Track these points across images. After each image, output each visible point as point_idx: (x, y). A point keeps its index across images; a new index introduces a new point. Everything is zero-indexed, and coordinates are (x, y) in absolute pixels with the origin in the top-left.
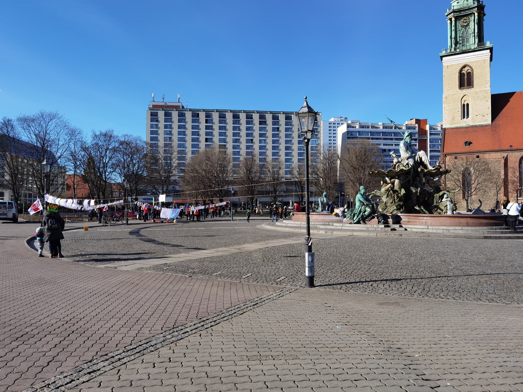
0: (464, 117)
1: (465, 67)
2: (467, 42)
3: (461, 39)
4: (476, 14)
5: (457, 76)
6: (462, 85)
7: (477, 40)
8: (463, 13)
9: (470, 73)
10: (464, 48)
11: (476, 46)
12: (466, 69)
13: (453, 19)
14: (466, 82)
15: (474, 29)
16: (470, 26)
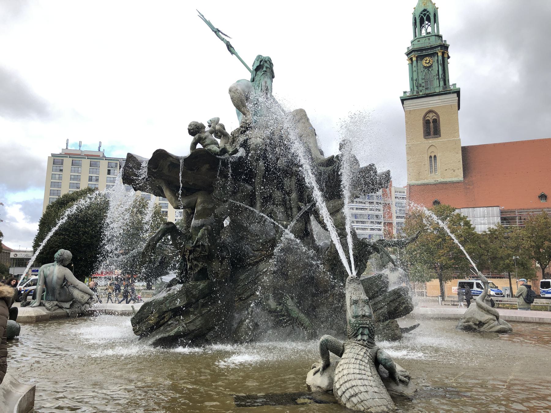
1: (430, 111)
5: (421, 122)
7: (442, 83)
8: (424, 53)
10: (428, 92)
11: (441, 89)
12: (431, 115)
13: (414, 59)
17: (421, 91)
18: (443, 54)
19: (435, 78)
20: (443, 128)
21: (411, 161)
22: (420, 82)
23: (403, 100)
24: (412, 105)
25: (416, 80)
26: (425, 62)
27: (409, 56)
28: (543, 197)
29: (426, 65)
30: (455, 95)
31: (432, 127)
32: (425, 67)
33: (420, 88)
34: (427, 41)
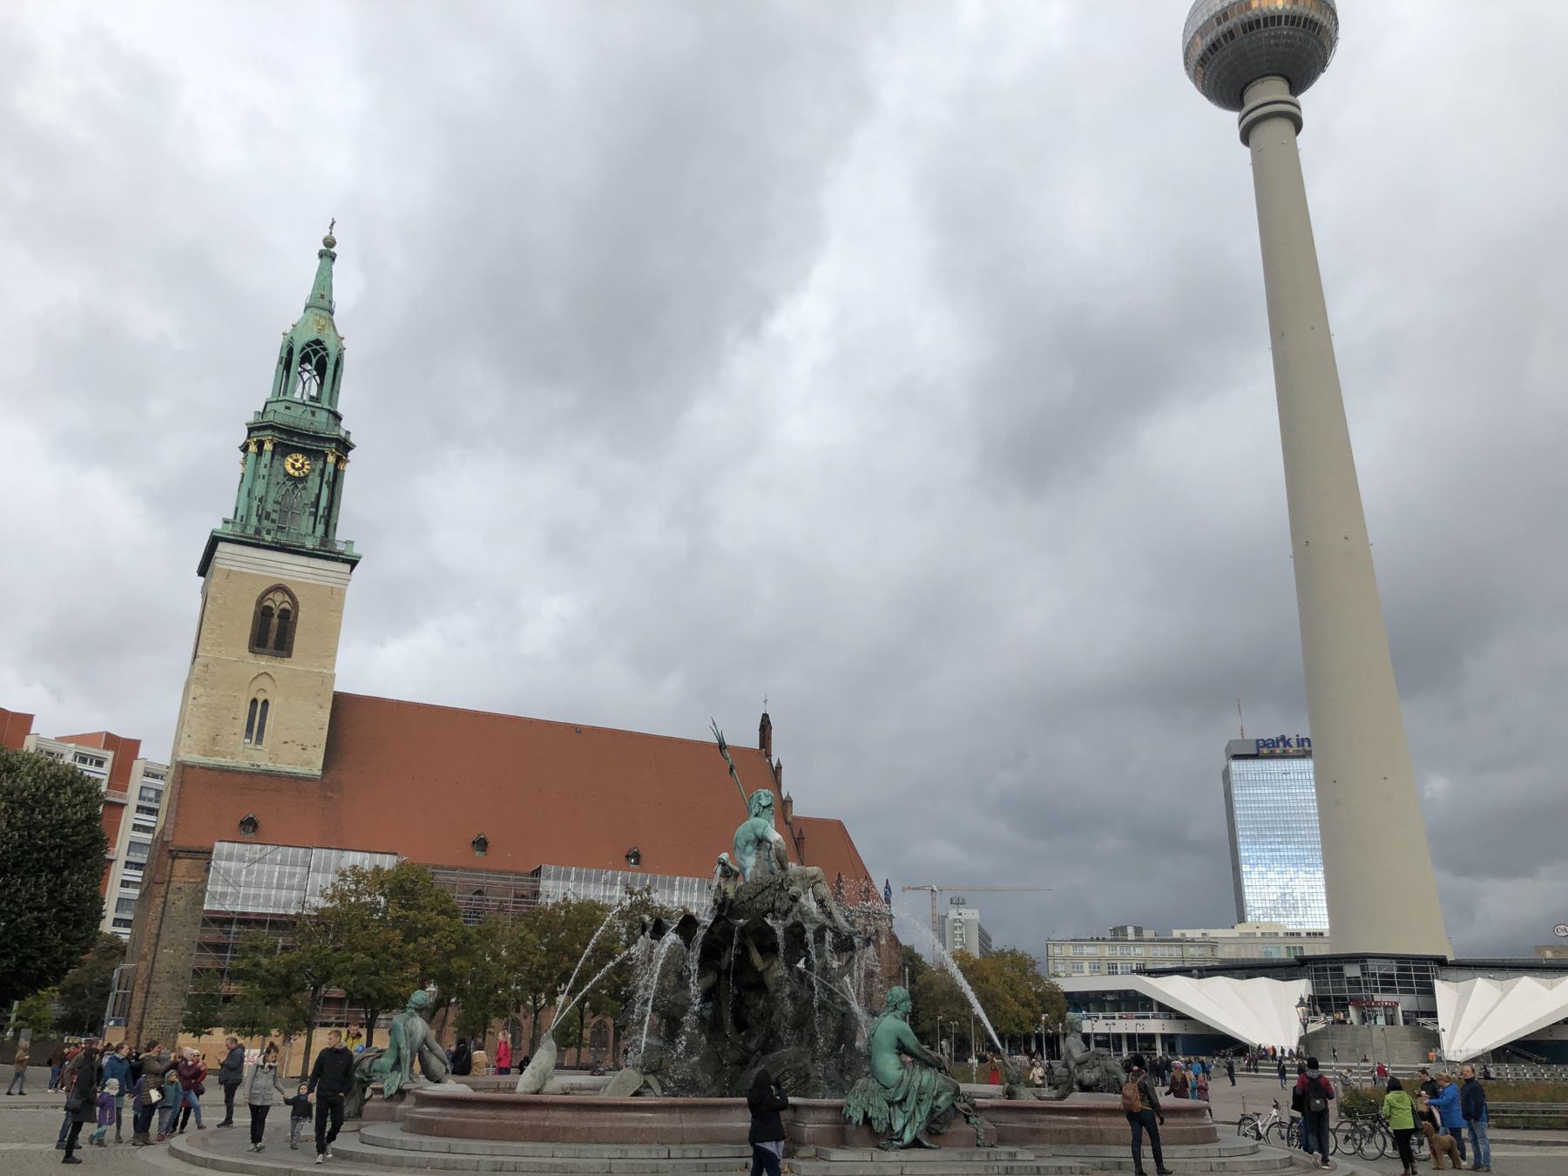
1: (280, 588)
6: (259, 642)
7: (320, 529)
10: (282, 538)
13: (268, 447)
14: (273, 636)
15: (318, 496)
16: (309, 484)
17: (268, 533)
18: (339, 460)
20: (300, 640)
21: (201, 700)
22: (270, 507)
23: (214, 541)
25: (261, 500)
26: (294, 464)
27: (255, 433)
28: (481, 844)
29: (292, 471)
31: (274, 629)
32: (287, 474)
33: (266, 523)
34: (308, 416)
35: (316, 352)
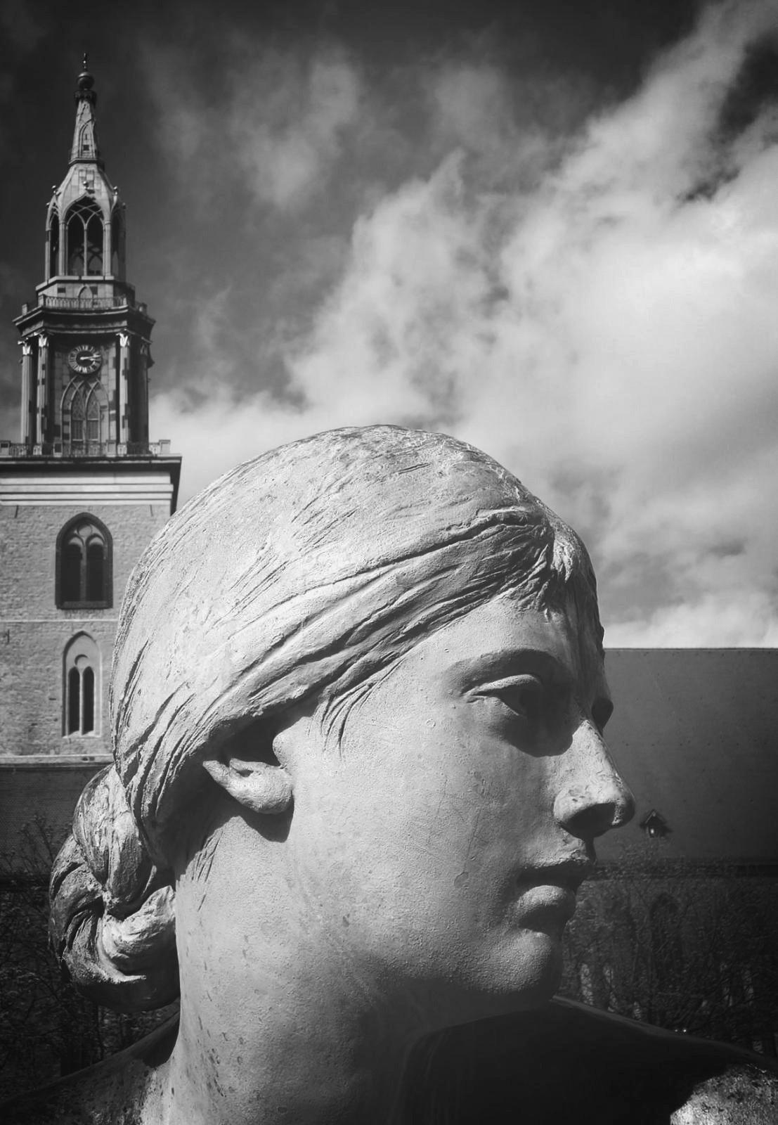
0: (74, 728)
1: (84, 519)
2: (93, 427)
3: (68, 418)
4: (124, 341)
5: (52, 549)
9: (96, 546)
11: (123, 451)
12: (85, 532)
14: (83, 583)
16: (103, 380)
17: (58, 450)
19: (106, 414)
20: (122, 584)
24: (24, 489)
29: (79, 368)
30: (166, 479)
32: (74, 374)
34: (88, 294)
35: (86, 215)
